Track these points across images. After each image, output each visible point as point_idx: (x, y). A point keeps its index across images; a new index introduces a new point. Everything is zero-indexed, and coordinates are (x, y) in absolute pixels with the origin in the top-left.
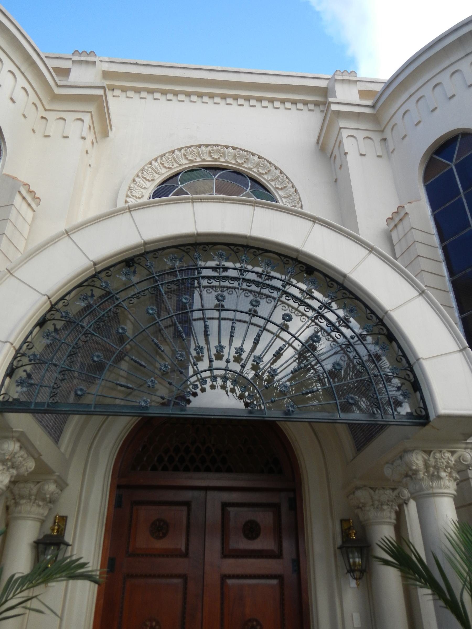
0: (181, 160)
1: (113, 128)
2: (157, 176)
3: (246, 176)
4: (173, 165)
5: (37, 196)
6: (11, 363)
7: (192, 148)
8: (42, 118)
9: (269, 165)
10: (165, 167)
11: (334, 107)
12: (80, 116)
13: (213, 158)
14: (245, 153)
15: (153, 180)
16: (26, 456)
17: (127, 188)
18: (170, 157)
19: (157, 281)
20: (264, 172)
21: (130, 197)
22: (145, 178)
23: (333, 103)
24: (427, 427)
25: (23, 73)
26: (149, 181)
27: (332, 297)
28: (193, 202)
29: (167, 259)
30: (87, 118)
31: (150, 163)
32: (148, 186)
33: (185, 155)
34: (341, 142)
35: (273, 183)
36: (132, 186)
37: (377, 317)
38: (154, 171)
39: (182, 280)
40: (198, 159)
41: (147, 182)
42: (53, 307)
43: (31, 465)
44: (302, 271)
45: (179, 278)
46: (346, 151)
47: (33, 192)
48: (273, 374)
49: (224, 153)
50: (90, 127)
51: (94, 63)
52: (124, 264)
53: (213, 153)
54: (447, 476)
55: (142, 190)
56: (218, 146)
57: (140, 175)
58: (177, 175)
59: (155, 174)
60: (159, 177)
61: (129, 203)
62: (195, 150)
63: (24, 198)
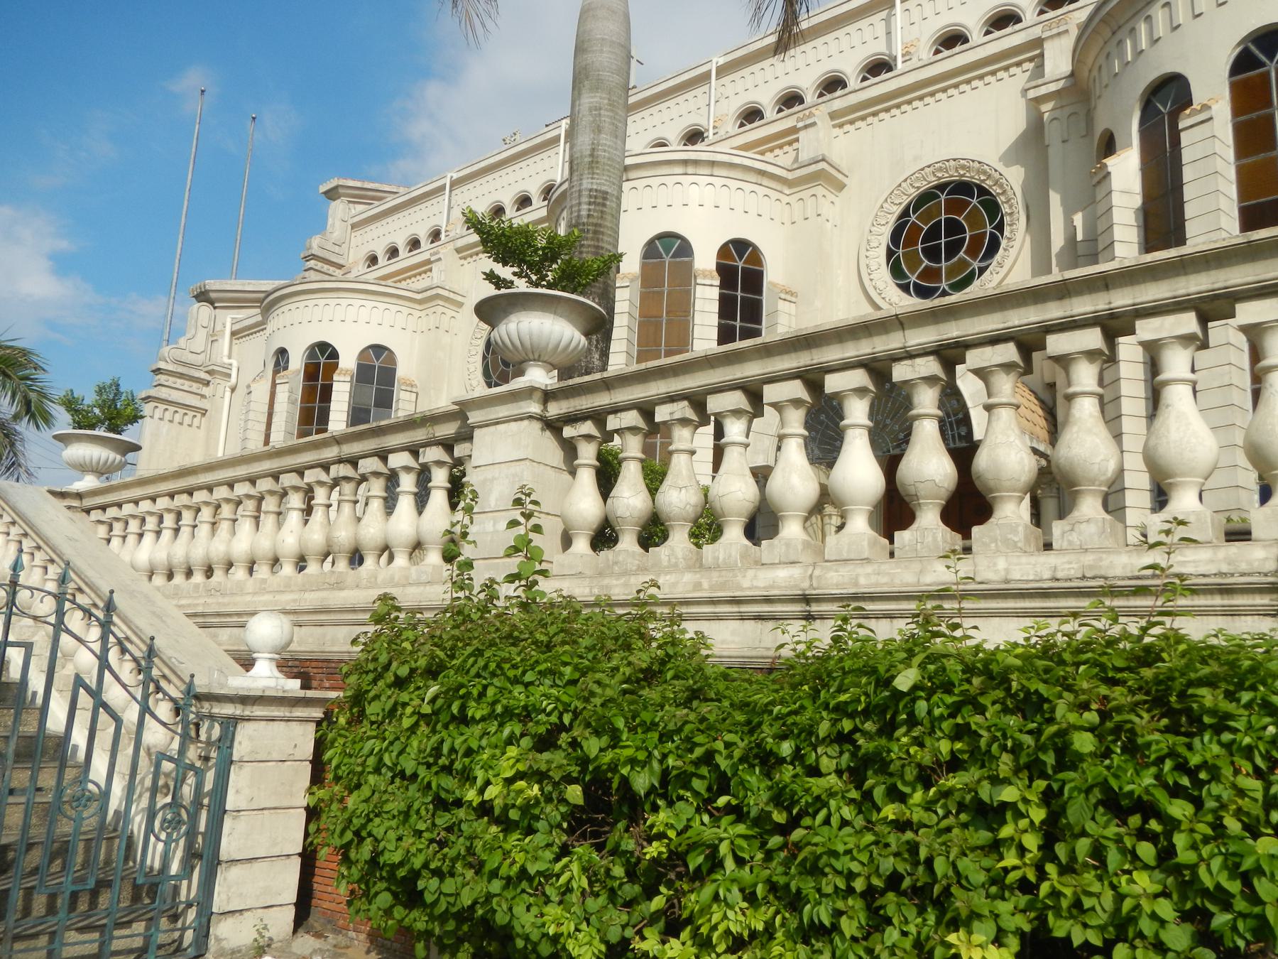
2: (889, 216)
40: (925, 183)
51: (814, 124)
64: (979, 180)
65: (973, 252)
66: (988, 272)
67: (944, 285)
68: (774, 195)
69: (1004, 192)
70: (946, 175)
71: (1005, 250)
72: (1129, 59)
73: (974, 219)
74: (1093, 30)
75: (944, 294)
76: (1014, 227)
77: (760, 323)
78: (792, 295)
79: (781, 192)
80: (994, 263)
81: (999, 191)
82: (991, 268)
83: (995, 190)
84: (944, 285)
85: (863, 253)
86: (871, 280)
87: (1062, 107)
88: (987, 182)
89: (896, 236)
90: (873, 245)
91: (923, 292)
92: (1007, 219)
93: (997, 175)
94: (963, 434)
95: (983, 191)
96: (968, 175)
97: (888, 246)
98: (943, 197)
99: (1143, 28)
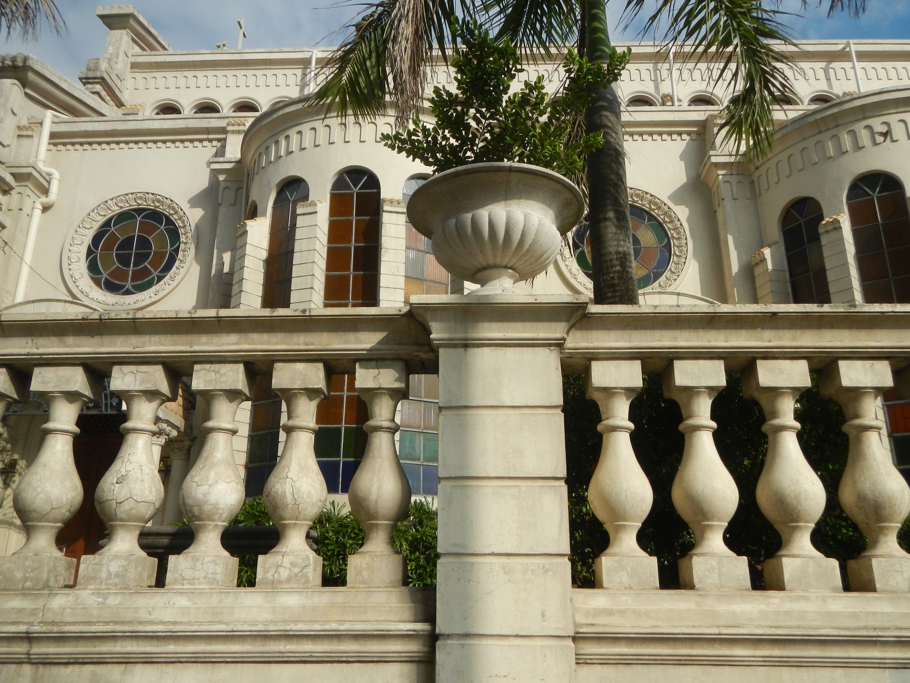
10: (102, 215)
26: (88, 229)
33: (116, 204)
35: (178, 221)
49: (145, 199)
55: (83, 237)
58: (110, 220)
64: (169, 213)
65: (155, 265)
66: (162, 282)
67: (129, 285)
69: (184, 226)
70: (145, 203)
71: (177, 268)
72: (272, 160)
73: (161, 241)
75: (128, 292)
76: (186, 253)
80: (168, 277)
81: (181, 224)
82: (165, 279)
83: (179, 223)
84: (129, 285)
85: (67, 246)
86: (70, 269)
89: (96, 239)
91: (111, 287)
92: (182, 246)
93: (181, 213)
94: (114, 404)
95: (169, 222)
96: (161, 207)
97: (89, 246)
98: (139, 219)
99: (283, 143)
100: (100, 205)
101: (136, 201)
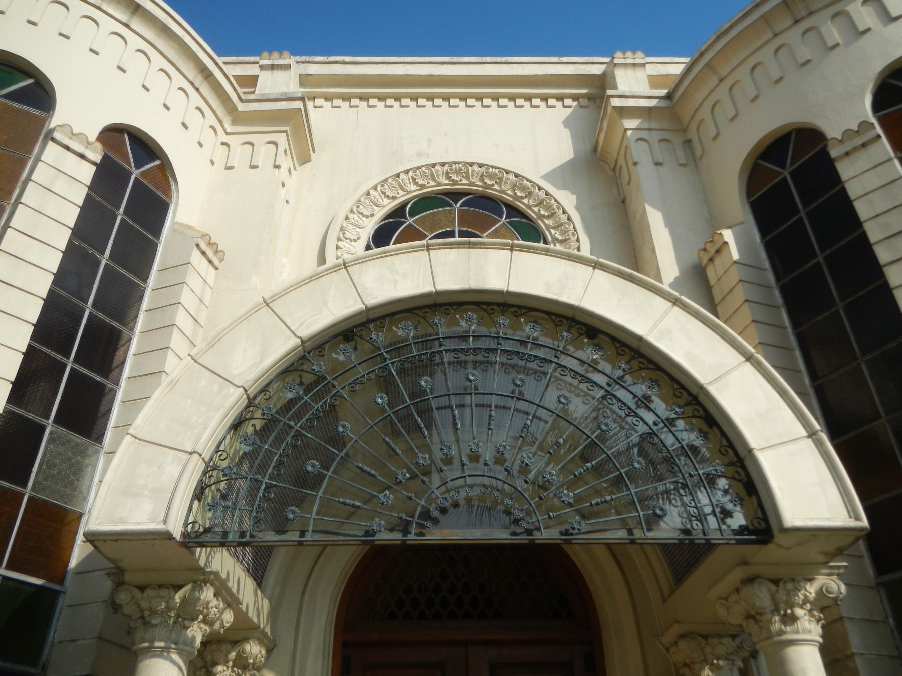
0: (409, 186)
1: (316, 150)
3: (499, 202)
4: (398, 193)
5: (220, 249)
6: (201, 481)
7: (424, 169)
8: (223, 144)
9: (529, 184)
10: (388, 197)
11: (615, 102)
12: (272, 137)
13: (453, 180)
14: (496, 171)
15: (372, 215)
16: (222, 605)
17: (338, 228)
18: (394, 183)
19: (385, 359)
20: (524, 195)
21: (342, 241)
22: (362, 214)
23: (613, 96)
24: (771, 546)
25: (197, 89)
26: (367, 217)
27: (624, 369)
28: (428, 250)
29: (397, 328)
30: (281, 139)
31: (368, 194)
32: (366, 224)
33: (414, 179)
34: (627, 148)
36: (345, 225)
37: (689, 393)
38: (372, 202)
39: (420, 355)
41: (364, 219)
42: (251, 402)
43: (228, 617)
44: (581, 335)
45: (416, 353)
46: (636, 160)
47: (215, 244)
48: (549, 478)
49: (467, 173)
50: (285, 152)
52: (341, 337)
53: (452, 173)
54: (805, 615)
55: (358, 230)
56: (458, 163)
57: (355, 210)
58: (403, 206)
59: (375, 207)
60: (380, 211)
61: (341, 248)
62: (427, 171)
63: (203, 253)
68: (211, 119)
69: (552, 215)
70: (464, 181)
74: (762, 16)
77: (145, 279)
78: (216, 252)
79: (221, 122)
87: (650, 129)
88: (525, 201)
90: (348, 235)
93: (542, 194)
96: (496, 187)
100: (386, 180)
101: (449, 178)
